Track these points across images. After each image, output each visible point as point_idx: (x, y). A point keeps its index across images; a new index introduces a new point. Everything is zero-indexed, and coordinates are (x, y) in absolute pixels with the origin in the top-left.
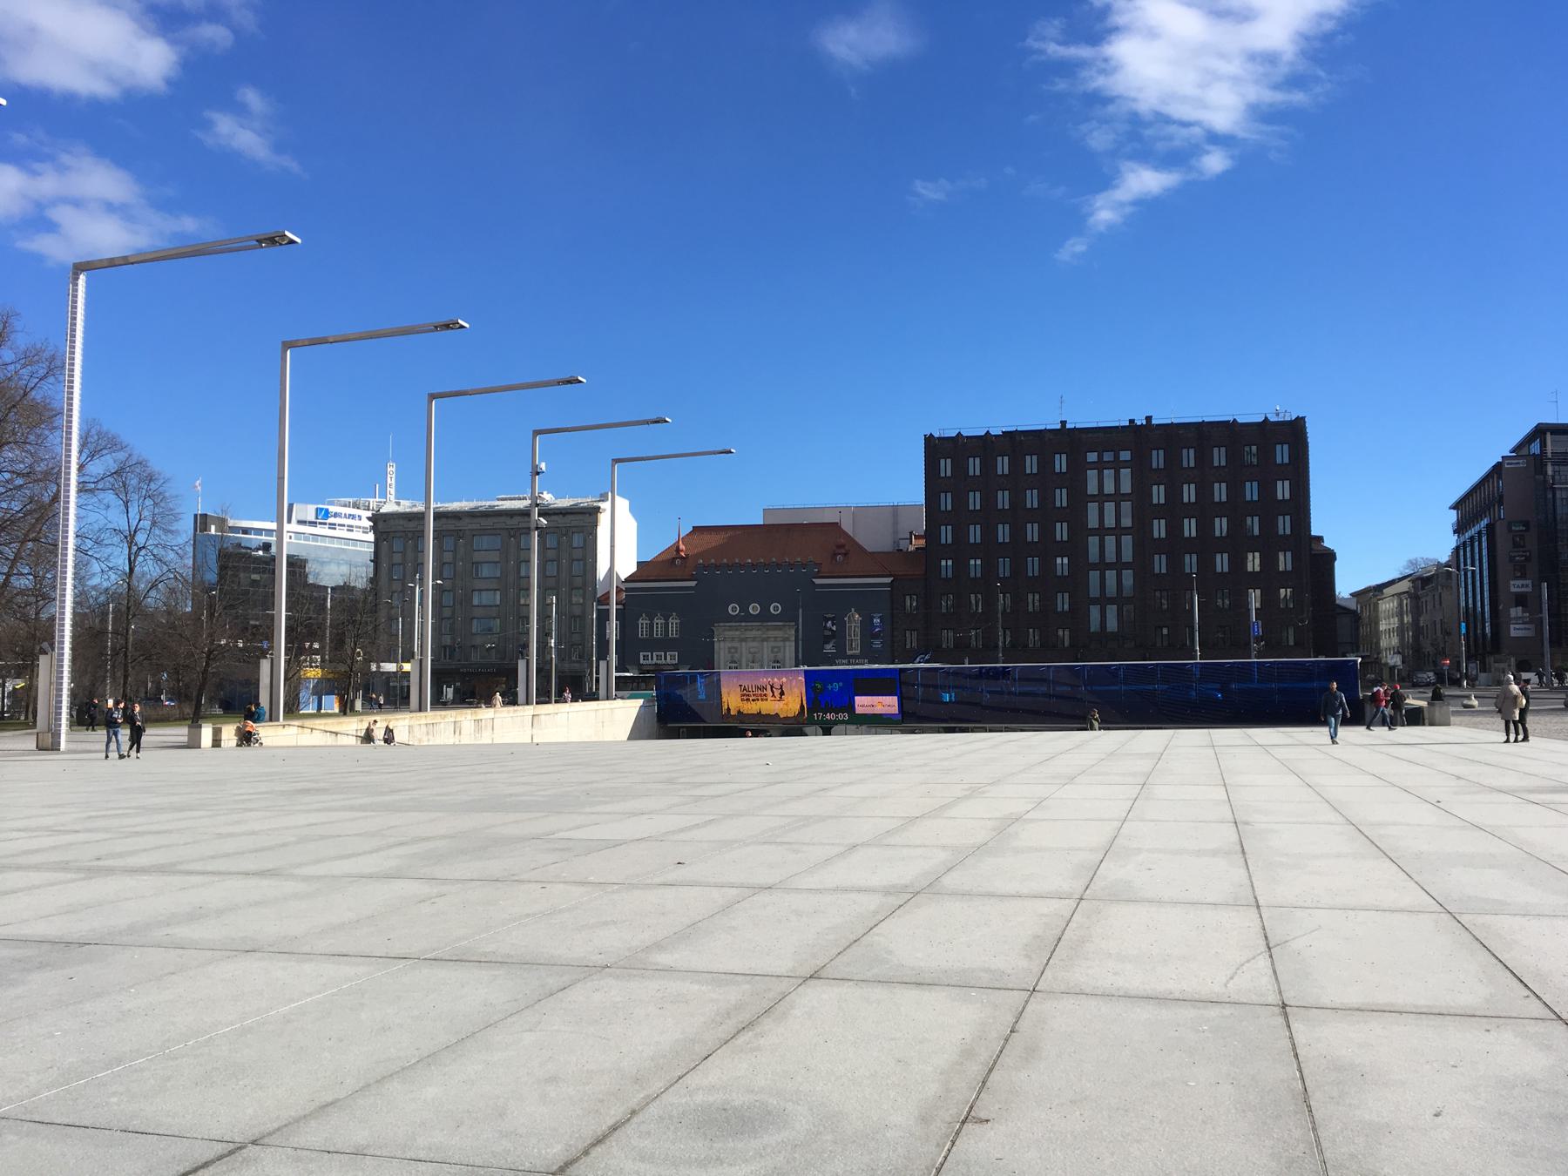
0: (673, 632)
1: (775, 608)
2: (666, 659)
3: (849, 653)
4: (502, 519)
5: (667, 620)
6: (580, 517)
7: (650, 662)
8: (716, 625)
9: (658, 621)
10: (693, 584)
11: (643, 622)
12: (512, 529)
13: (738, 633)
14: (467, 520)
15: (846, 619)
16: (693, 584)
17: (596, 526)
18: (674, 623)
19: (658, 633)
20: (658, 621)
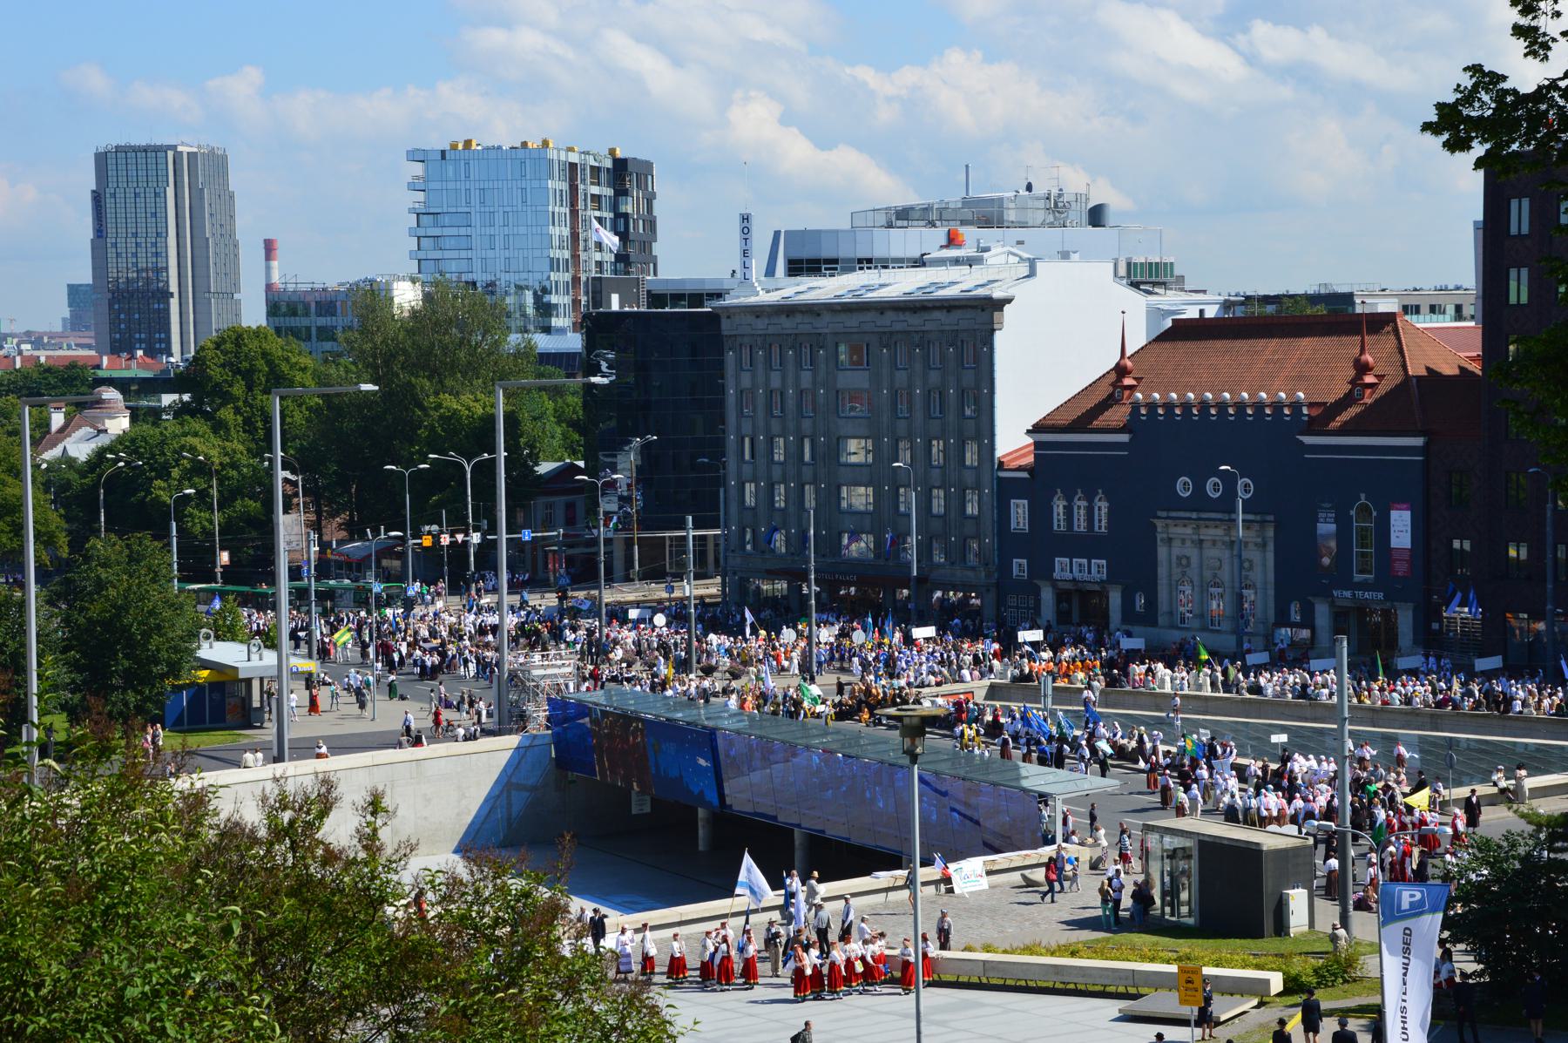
0: (1102, 524)
1: (1244, 488)
2: (1090, 572)
3: (1358, 577)
4: (869, 316)
5: (1090, 500)
6: (969, 314)
7: (1068, 576)
8: (1160, 513)
9: (1080, 504)
10: (1124, 438)
11: (1059, 506)
12: (885, 333)
13: (1189, 531)
14: (827, 317)
15: (1353, 513)
16: (1124, 438)
17: (993, 331)
18: (1102, 507)
19: (1080, 525)
20: (1080, 504)
